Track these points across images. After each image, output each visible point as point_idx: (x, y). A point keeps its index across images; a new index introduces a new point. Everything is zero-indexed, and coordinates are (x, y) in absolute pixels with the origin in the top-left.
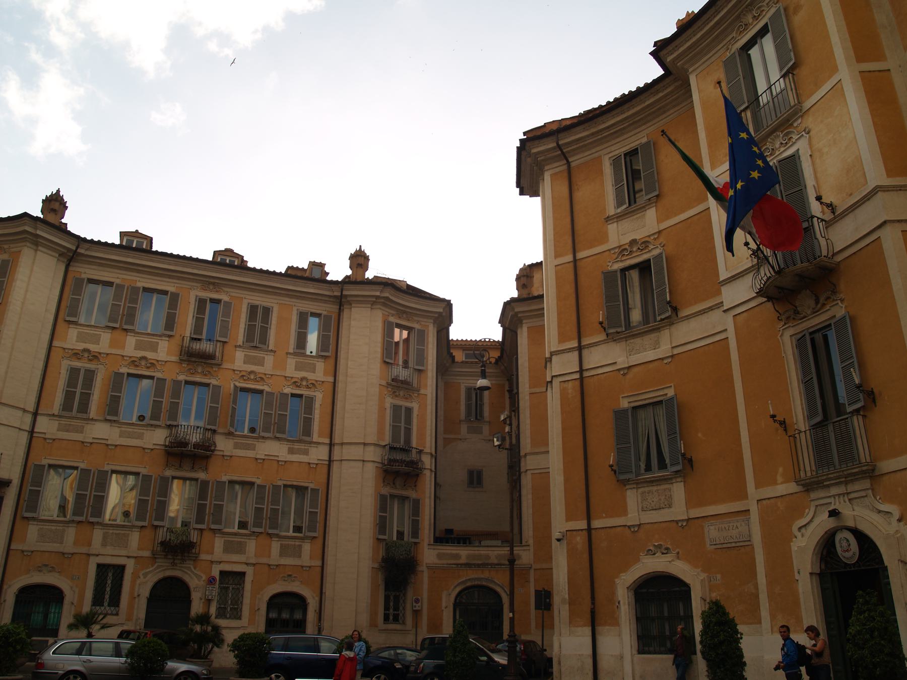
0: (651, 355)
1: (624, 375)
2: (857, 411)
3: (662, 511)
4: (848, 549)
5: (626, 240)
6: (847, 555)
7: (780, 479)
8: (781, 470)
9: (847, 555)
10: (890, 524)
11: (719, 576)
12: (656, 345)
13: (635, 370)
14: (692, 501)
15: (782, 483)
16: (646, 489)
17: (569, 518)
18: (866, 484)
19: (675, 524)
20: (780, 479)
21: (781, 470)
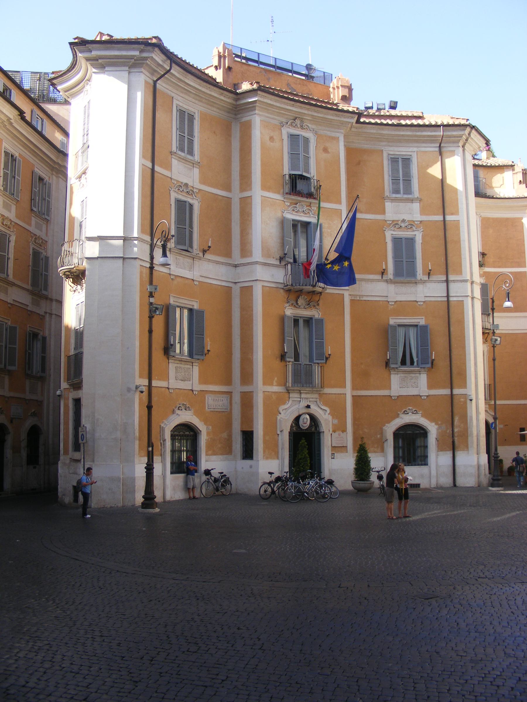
0: (187, 274)
1: (172, 279)
2: (318, 363)
3: (186, 382)
4: (305, 423)
5: (185, 181)
6: (305, 425)
7: (275, 383)
8: (276, 379)
9: (305, 425)
10: (325, 414)
11: (210, 427)
12: (191, 268)
13: (179, 279)
14: (203, 380)
15: (275, 386)
16: (179, 365)
17: (141, 376)
18: (316, 396)
19: (191, 391)
20: (275, 383)
21: (276, 379)
